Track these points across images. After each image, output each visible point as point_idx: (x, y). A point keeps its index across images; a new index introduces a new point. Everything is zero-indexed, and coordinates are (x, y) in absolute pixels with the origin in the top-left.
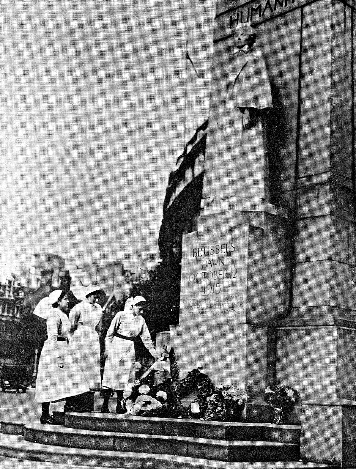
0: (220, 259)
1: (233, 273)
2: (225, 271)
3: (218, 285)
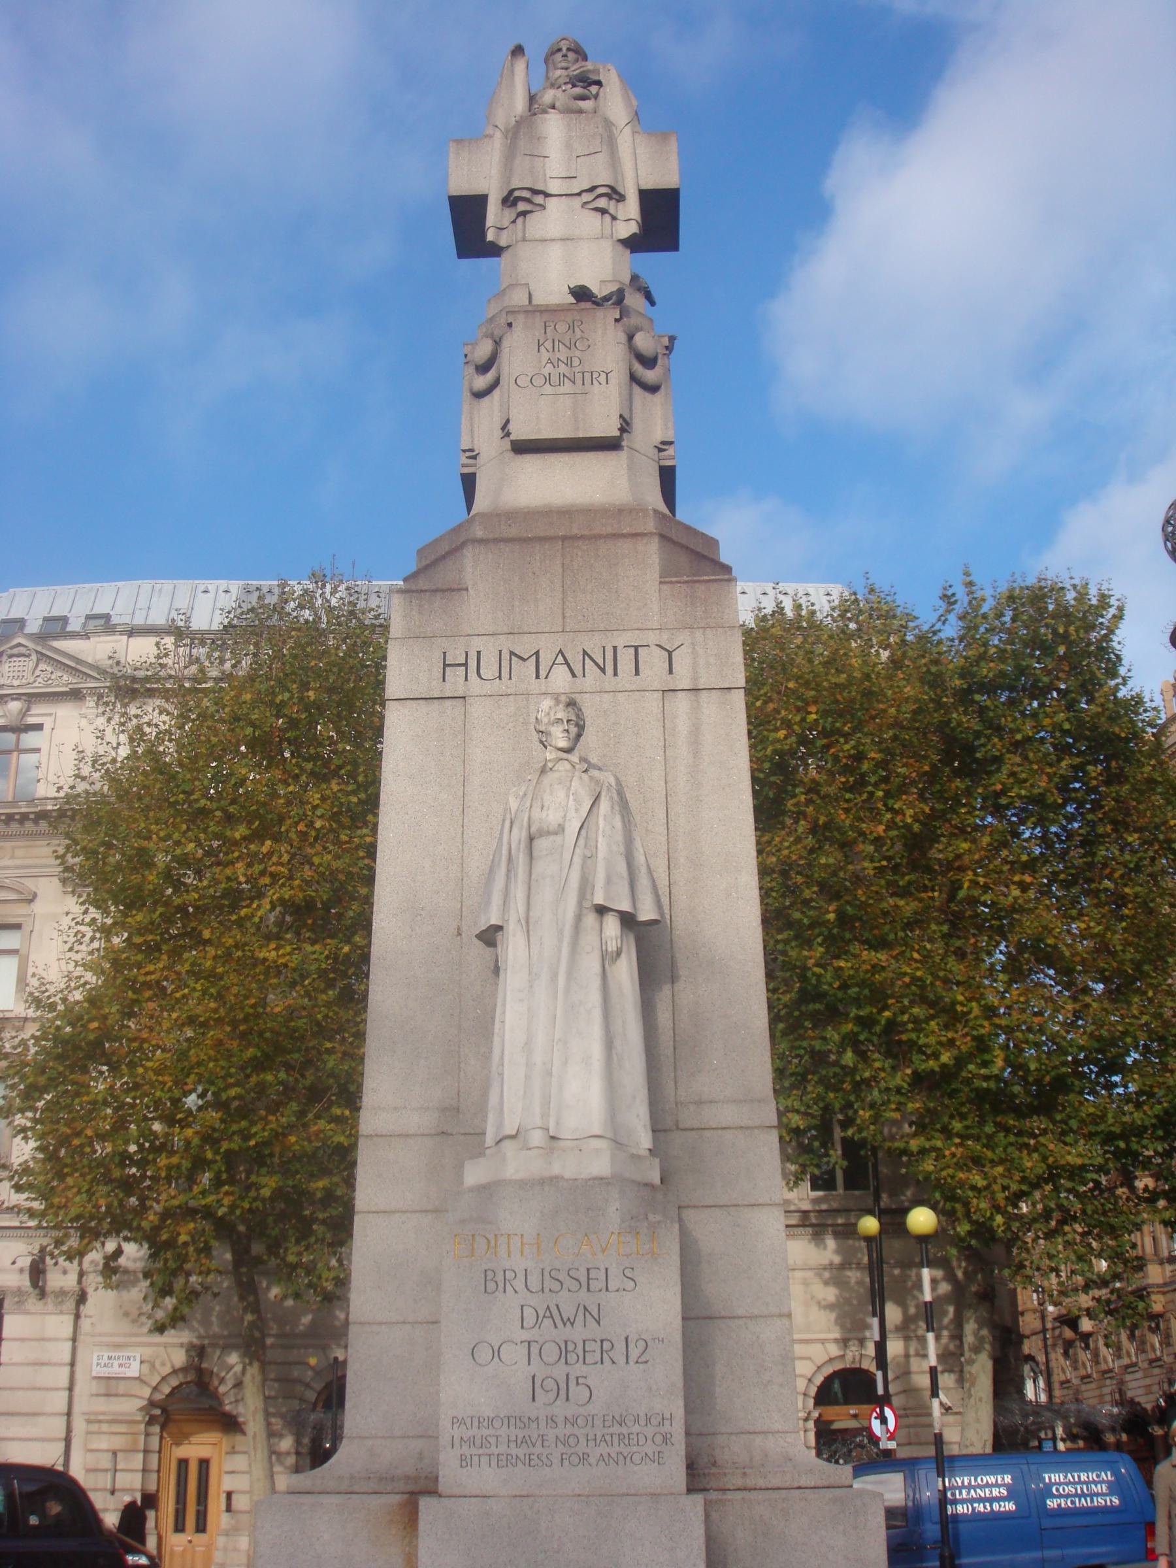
0: (585, 1308)
1: (634, 1353)
2: (606, 1345)
3: (581, 1381)
